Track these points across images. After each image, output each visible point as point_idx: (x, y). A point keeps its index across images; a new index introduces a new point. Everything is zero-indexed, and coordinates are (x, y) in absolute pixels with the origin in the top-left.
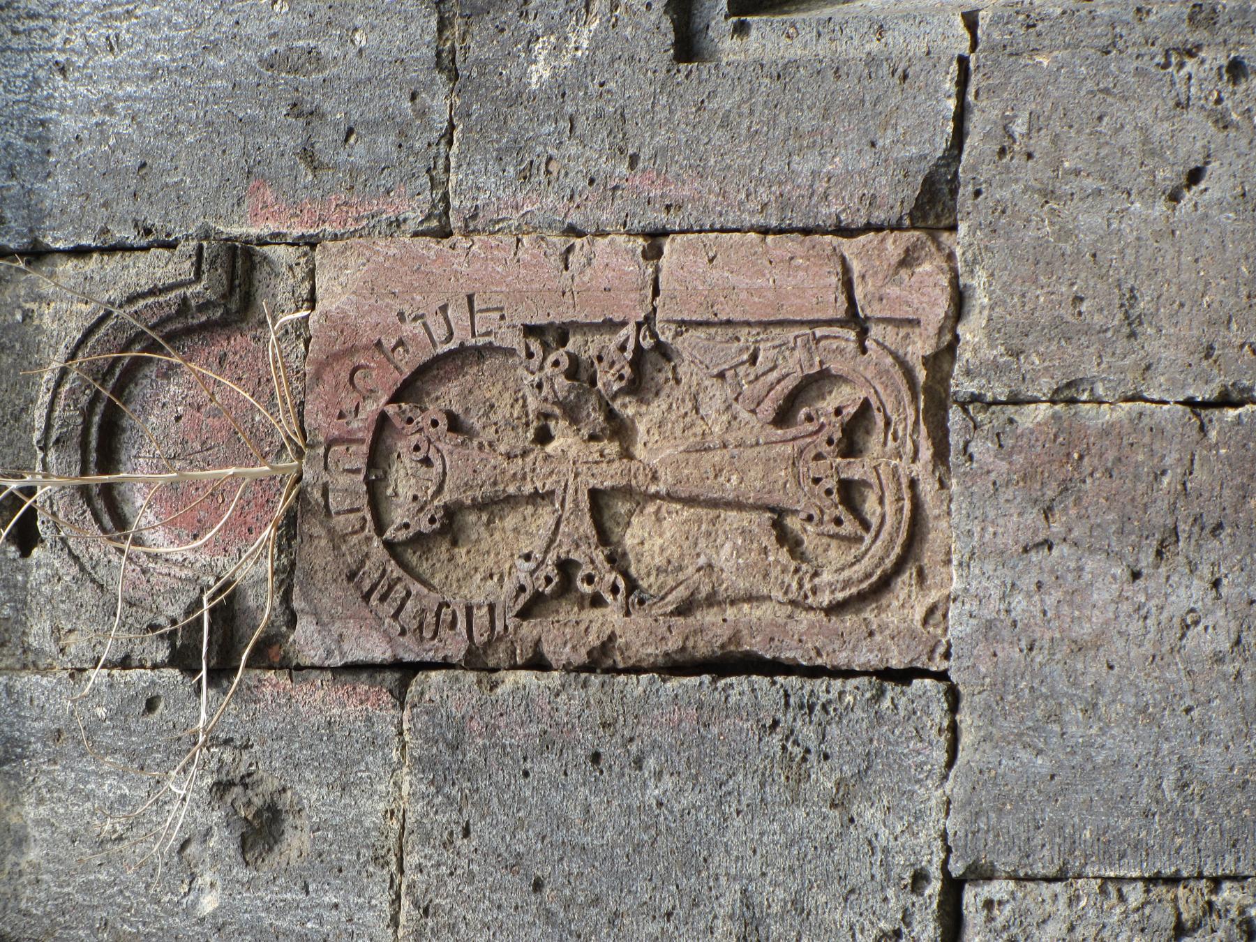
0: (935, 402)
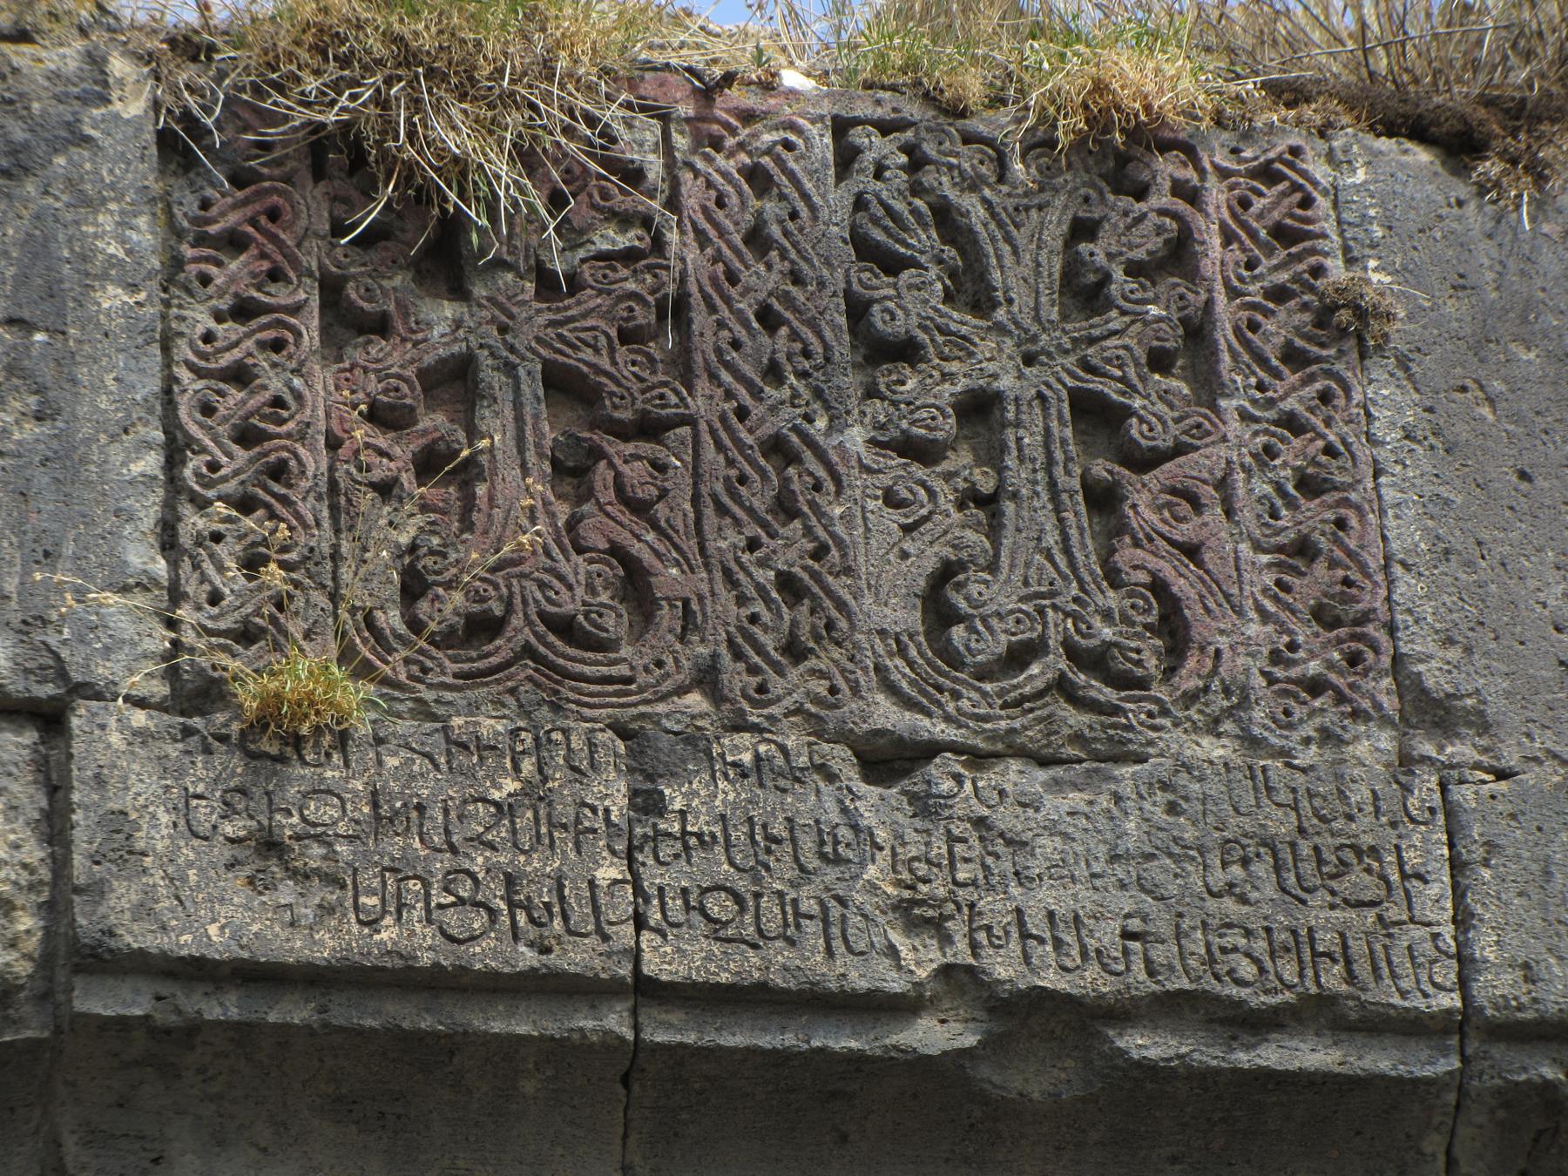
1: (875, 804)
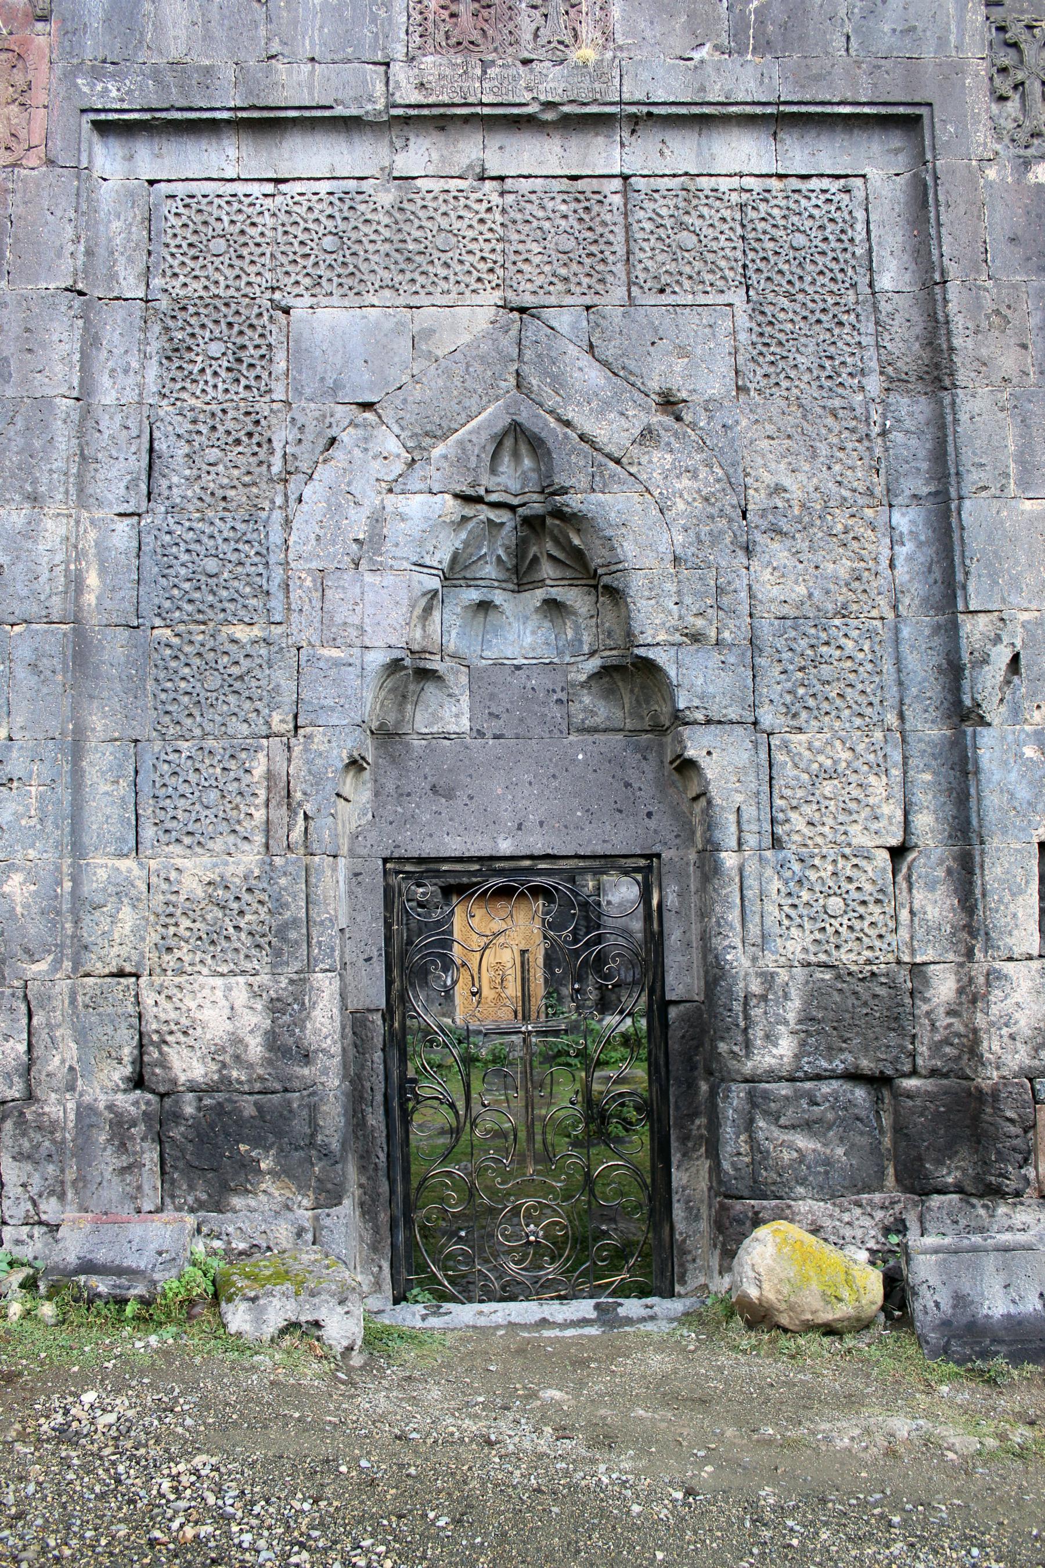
1: (522, 69)
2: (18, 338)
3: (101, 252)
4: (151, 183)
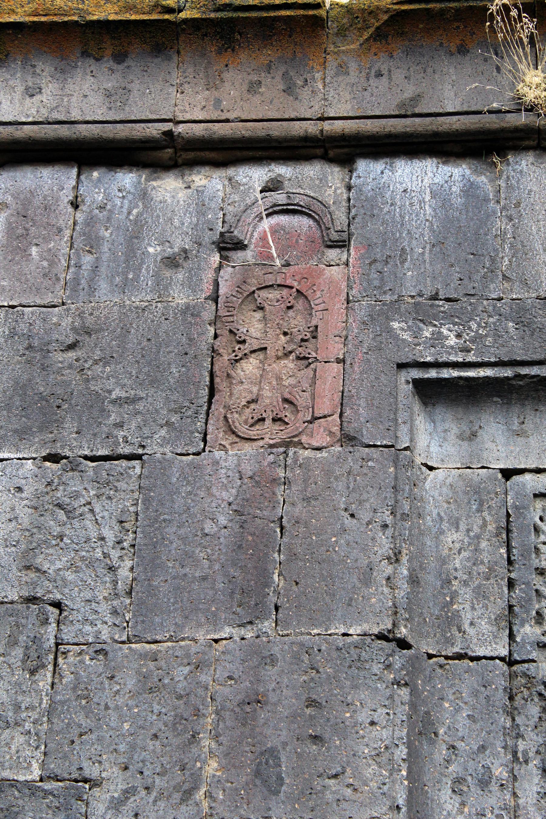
0: (287, 444)
2: (294, 716)
3: (430, 579)
4: (508, 474)
